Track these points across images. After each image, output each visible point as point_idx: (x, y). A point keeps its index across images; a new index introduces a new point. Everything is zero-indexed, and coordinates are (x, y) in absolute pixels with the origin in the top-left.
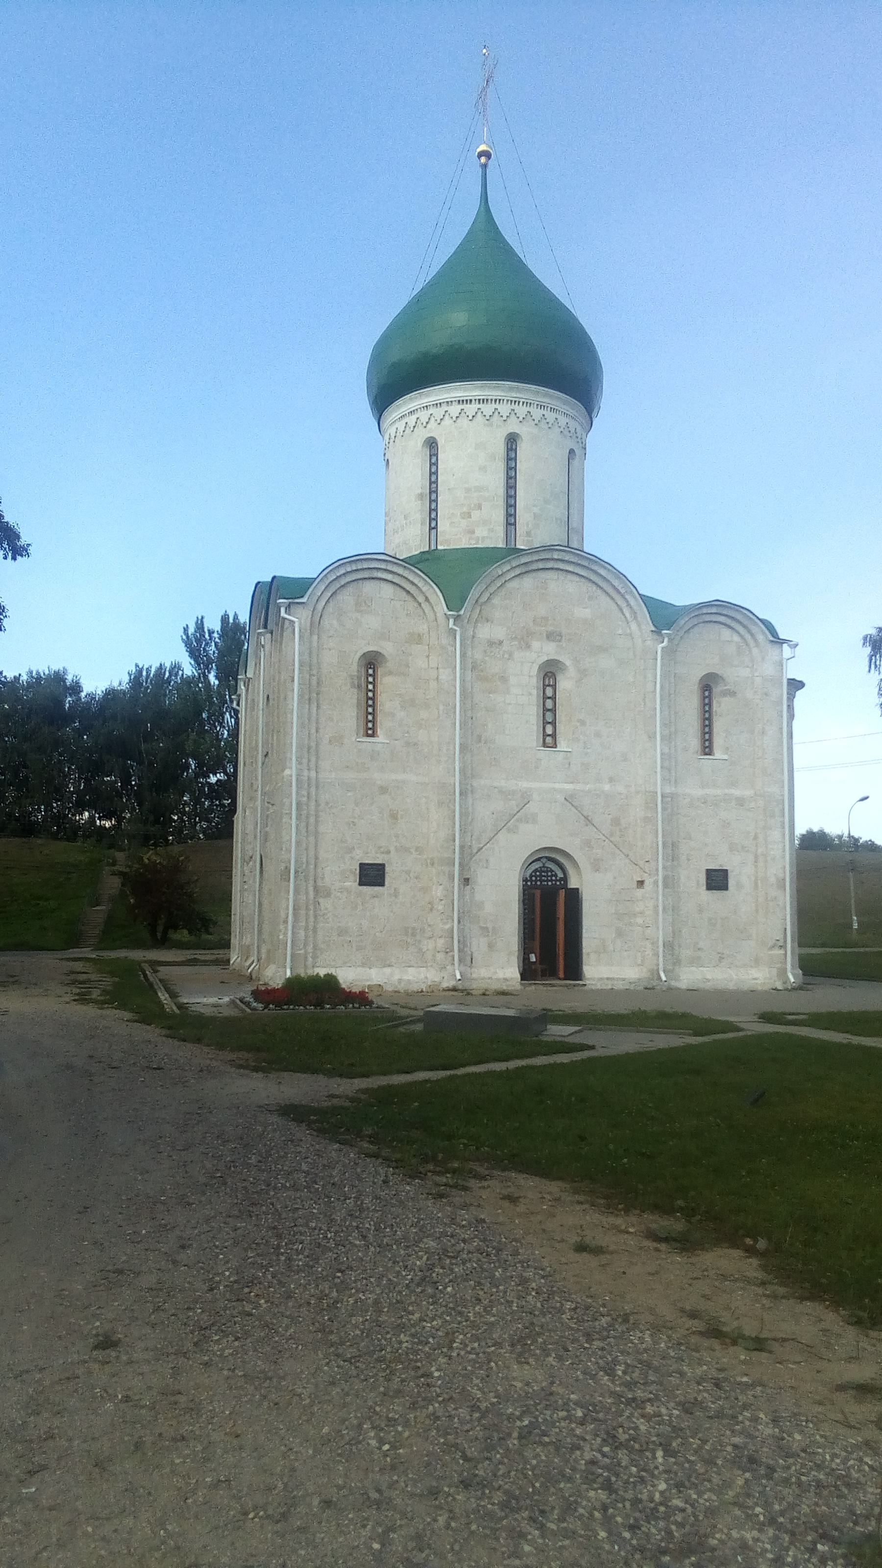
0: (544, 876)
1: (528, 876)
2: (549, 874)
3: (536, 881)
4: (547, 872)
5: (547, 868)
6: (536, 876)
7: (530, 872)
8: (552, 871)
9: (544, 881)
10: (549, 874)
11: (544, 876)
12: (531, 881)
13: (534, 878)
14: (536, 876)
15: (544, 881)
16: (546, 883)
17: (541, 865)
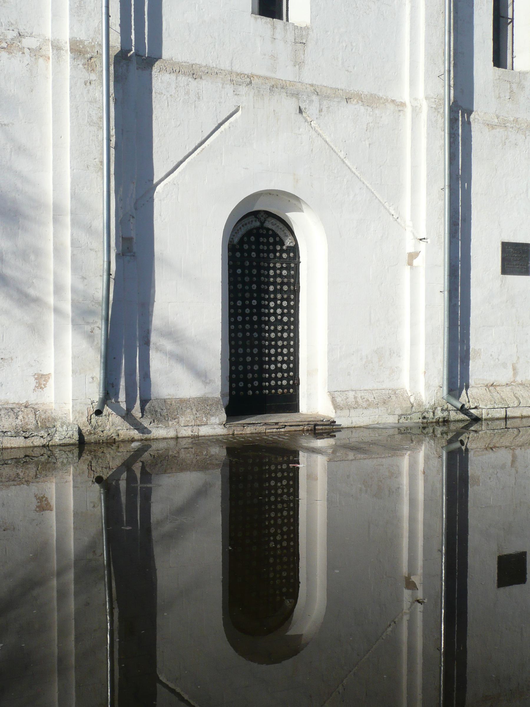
0: (263, 243)
1: (236, 240)
2: (271, 240)
3: (250, 251)
4: (267, 236)
5: (268, 229)
6: (249, 243)
7: (240, 235)
8: (275, 235)
9: (263, 251)
10: (271, 240)
11: (263, 243)
12: (242, 251)
13: (246, 247)
14: (249, 243)
15: (263, 251)
16: (265, 255)
17: (258, 224)
